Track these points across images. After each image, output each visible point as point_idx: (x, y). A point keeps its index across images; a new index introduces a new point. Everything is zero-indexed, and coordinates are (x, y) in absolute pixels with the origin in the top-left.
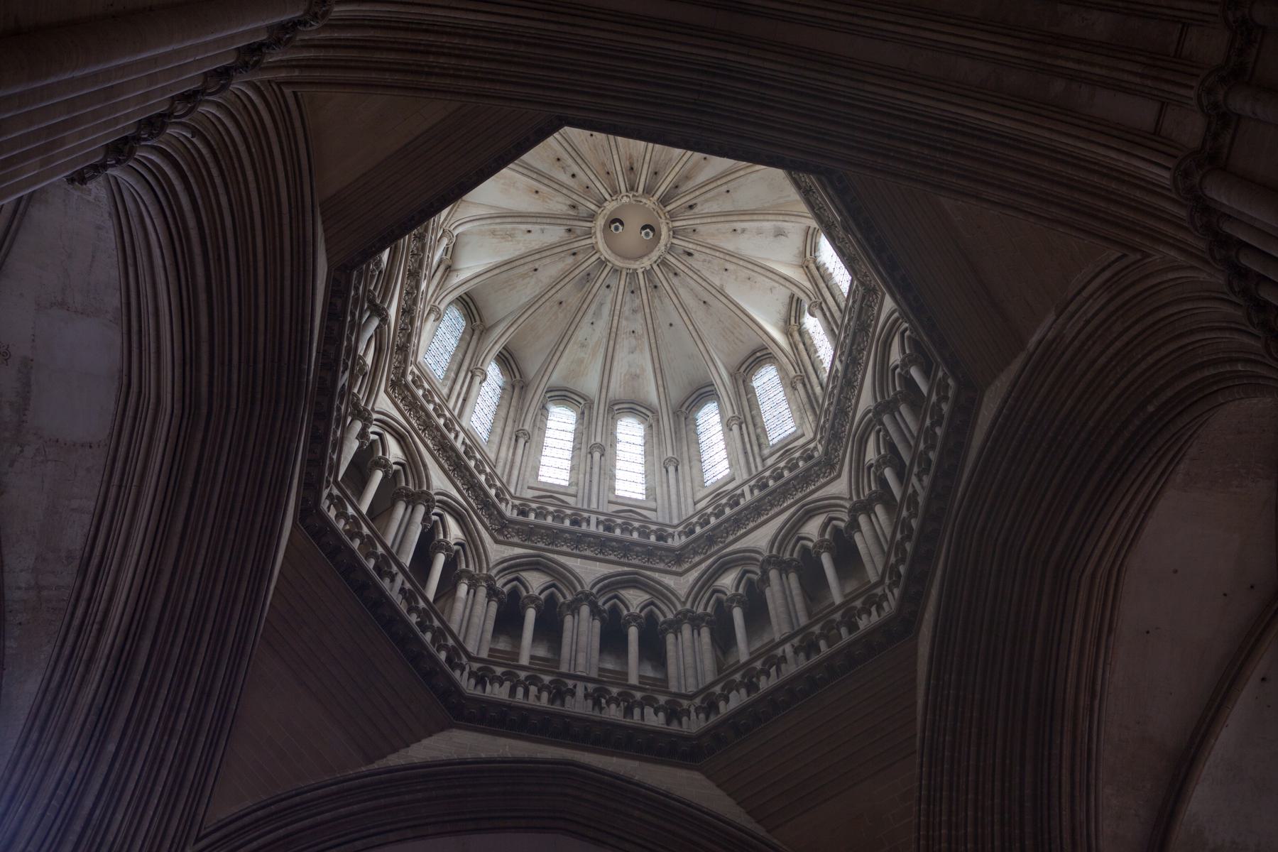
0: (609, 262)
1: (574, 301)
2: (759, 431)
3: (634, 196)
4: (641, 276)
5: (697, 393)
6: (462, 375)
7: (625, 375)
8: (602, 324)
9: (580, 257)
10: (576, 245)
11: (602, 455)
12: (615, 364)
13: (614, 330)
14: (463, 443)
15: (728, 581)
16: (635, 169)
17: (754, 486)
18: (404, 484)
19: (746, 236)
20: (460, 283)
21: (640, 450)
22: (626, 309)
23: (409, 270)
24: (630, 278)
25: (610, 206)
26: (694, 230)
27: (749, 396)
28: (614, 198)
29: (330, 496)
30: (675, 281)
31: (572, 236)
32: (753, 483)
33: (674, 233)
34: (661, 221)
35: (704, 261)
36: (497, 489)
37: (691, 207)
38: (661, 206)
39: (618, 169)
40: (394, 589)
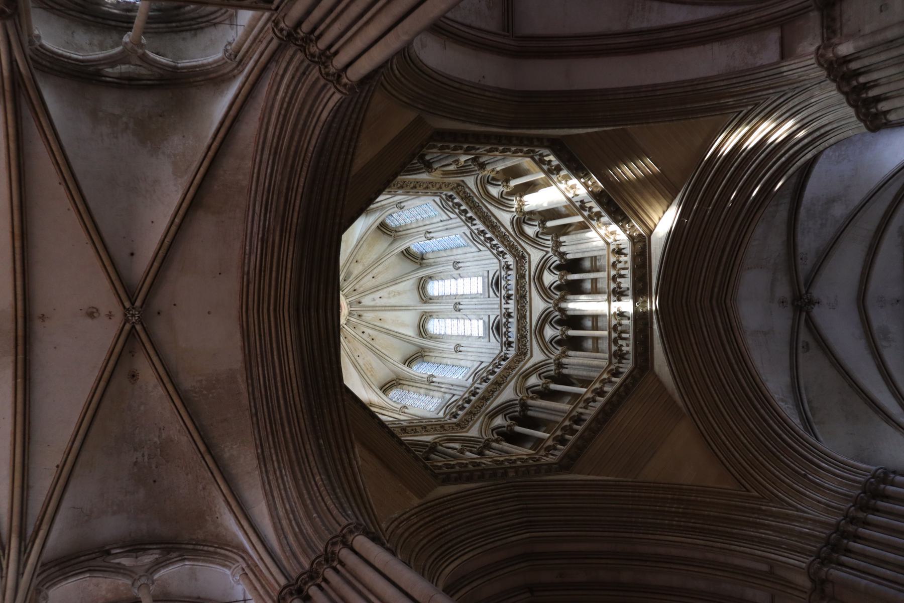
11: (459, 304)
14: (480, 384)
17: (472, 223)
18: (517, 413)
32: (470, 225)
36: (500, 361)
40: (590, 413)
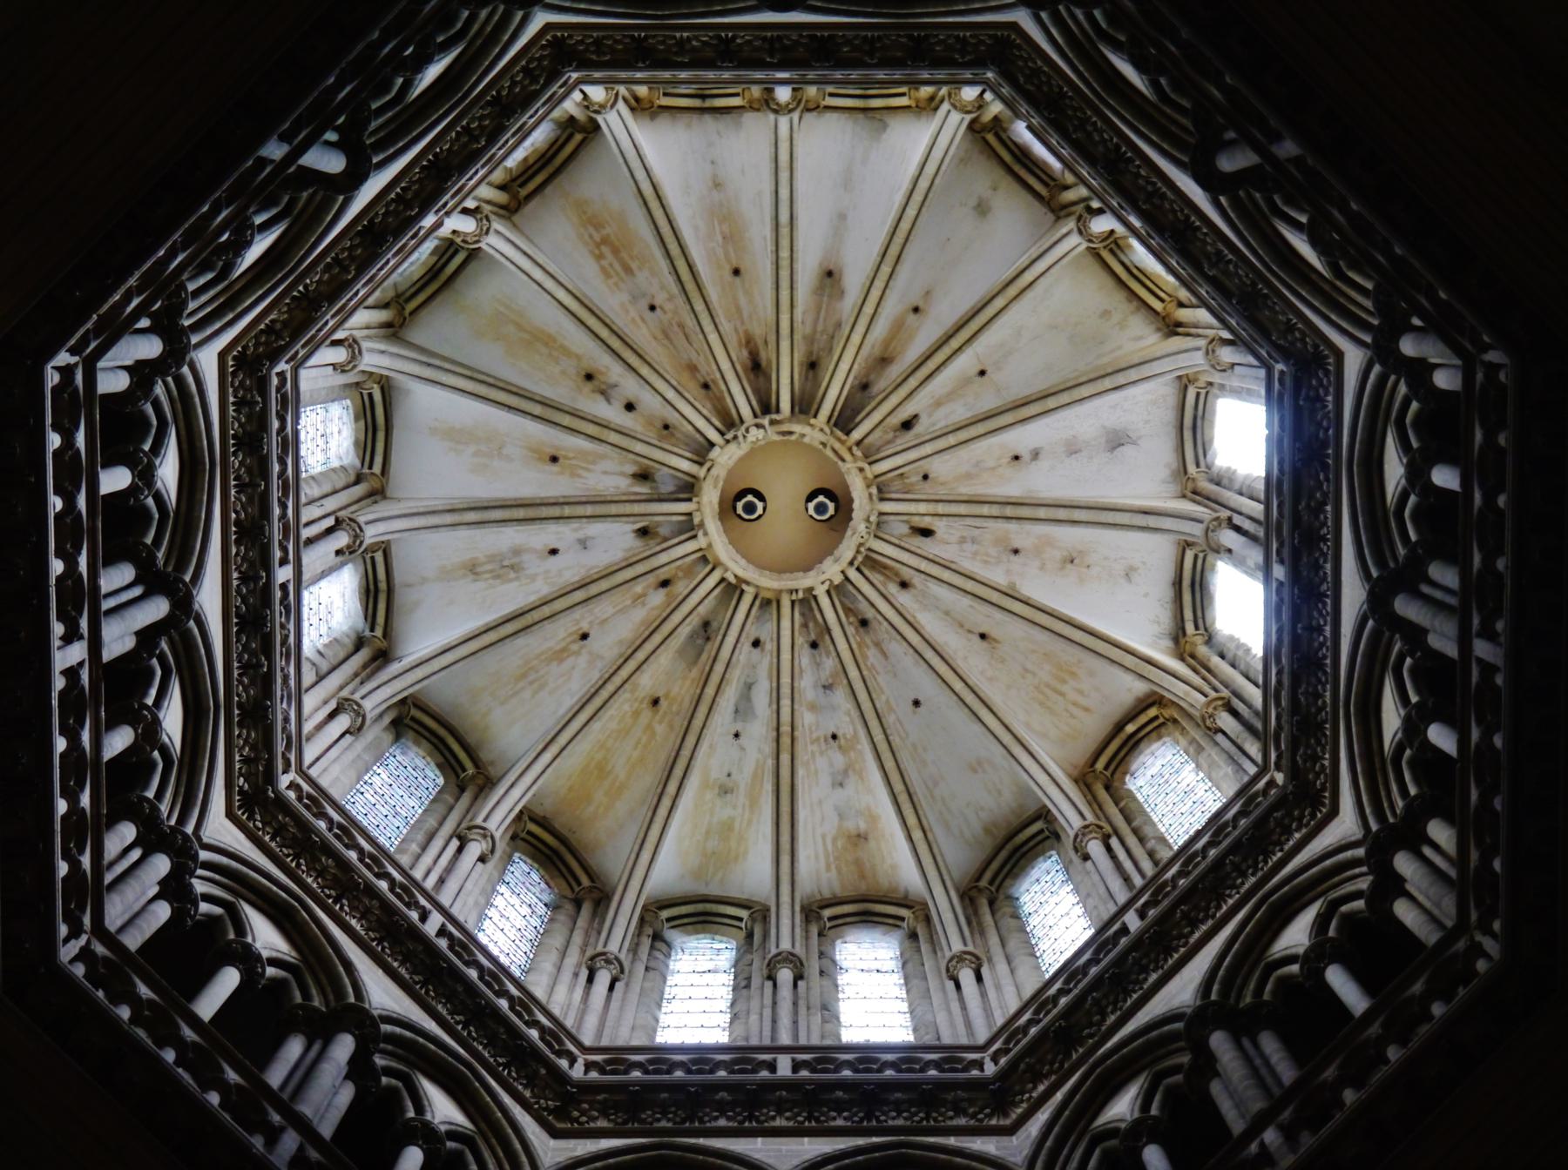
0: (748, 583)
1: (682, 690)
2: (1151, 844)
3: (772, 422)
4: (825, 602)
5: (1009, 847)
6: (437, 843)
7: (834, 840)
8: (758, 731)
9: (681, 588)
10: (664, 558)
11: (798, 977)
12: (802, 814)
13: (786, 728)
16: (764, 364)
19: (1043, 464)
20: (408, 667)
21: (897, 979)
22: (806, 684)
23: (238, 523)
24: (802, 614)
26: (925, 477)
27: (1122, 804)
28: (729, 436)
30: (903, 598)
31: (652, 542)
33: (880, 490)
34: (843, 467)
35: (962, 540)
37: (907, 425)
38: (839, 433)
39: (725, 365)
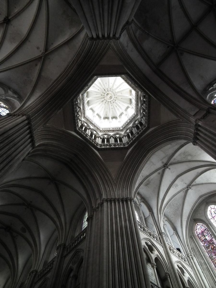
15: (128, 131)
25: (107, 93)
29: (78, 128)
40: (88, 137)
